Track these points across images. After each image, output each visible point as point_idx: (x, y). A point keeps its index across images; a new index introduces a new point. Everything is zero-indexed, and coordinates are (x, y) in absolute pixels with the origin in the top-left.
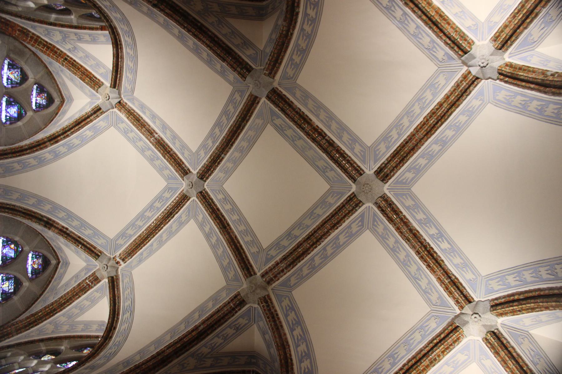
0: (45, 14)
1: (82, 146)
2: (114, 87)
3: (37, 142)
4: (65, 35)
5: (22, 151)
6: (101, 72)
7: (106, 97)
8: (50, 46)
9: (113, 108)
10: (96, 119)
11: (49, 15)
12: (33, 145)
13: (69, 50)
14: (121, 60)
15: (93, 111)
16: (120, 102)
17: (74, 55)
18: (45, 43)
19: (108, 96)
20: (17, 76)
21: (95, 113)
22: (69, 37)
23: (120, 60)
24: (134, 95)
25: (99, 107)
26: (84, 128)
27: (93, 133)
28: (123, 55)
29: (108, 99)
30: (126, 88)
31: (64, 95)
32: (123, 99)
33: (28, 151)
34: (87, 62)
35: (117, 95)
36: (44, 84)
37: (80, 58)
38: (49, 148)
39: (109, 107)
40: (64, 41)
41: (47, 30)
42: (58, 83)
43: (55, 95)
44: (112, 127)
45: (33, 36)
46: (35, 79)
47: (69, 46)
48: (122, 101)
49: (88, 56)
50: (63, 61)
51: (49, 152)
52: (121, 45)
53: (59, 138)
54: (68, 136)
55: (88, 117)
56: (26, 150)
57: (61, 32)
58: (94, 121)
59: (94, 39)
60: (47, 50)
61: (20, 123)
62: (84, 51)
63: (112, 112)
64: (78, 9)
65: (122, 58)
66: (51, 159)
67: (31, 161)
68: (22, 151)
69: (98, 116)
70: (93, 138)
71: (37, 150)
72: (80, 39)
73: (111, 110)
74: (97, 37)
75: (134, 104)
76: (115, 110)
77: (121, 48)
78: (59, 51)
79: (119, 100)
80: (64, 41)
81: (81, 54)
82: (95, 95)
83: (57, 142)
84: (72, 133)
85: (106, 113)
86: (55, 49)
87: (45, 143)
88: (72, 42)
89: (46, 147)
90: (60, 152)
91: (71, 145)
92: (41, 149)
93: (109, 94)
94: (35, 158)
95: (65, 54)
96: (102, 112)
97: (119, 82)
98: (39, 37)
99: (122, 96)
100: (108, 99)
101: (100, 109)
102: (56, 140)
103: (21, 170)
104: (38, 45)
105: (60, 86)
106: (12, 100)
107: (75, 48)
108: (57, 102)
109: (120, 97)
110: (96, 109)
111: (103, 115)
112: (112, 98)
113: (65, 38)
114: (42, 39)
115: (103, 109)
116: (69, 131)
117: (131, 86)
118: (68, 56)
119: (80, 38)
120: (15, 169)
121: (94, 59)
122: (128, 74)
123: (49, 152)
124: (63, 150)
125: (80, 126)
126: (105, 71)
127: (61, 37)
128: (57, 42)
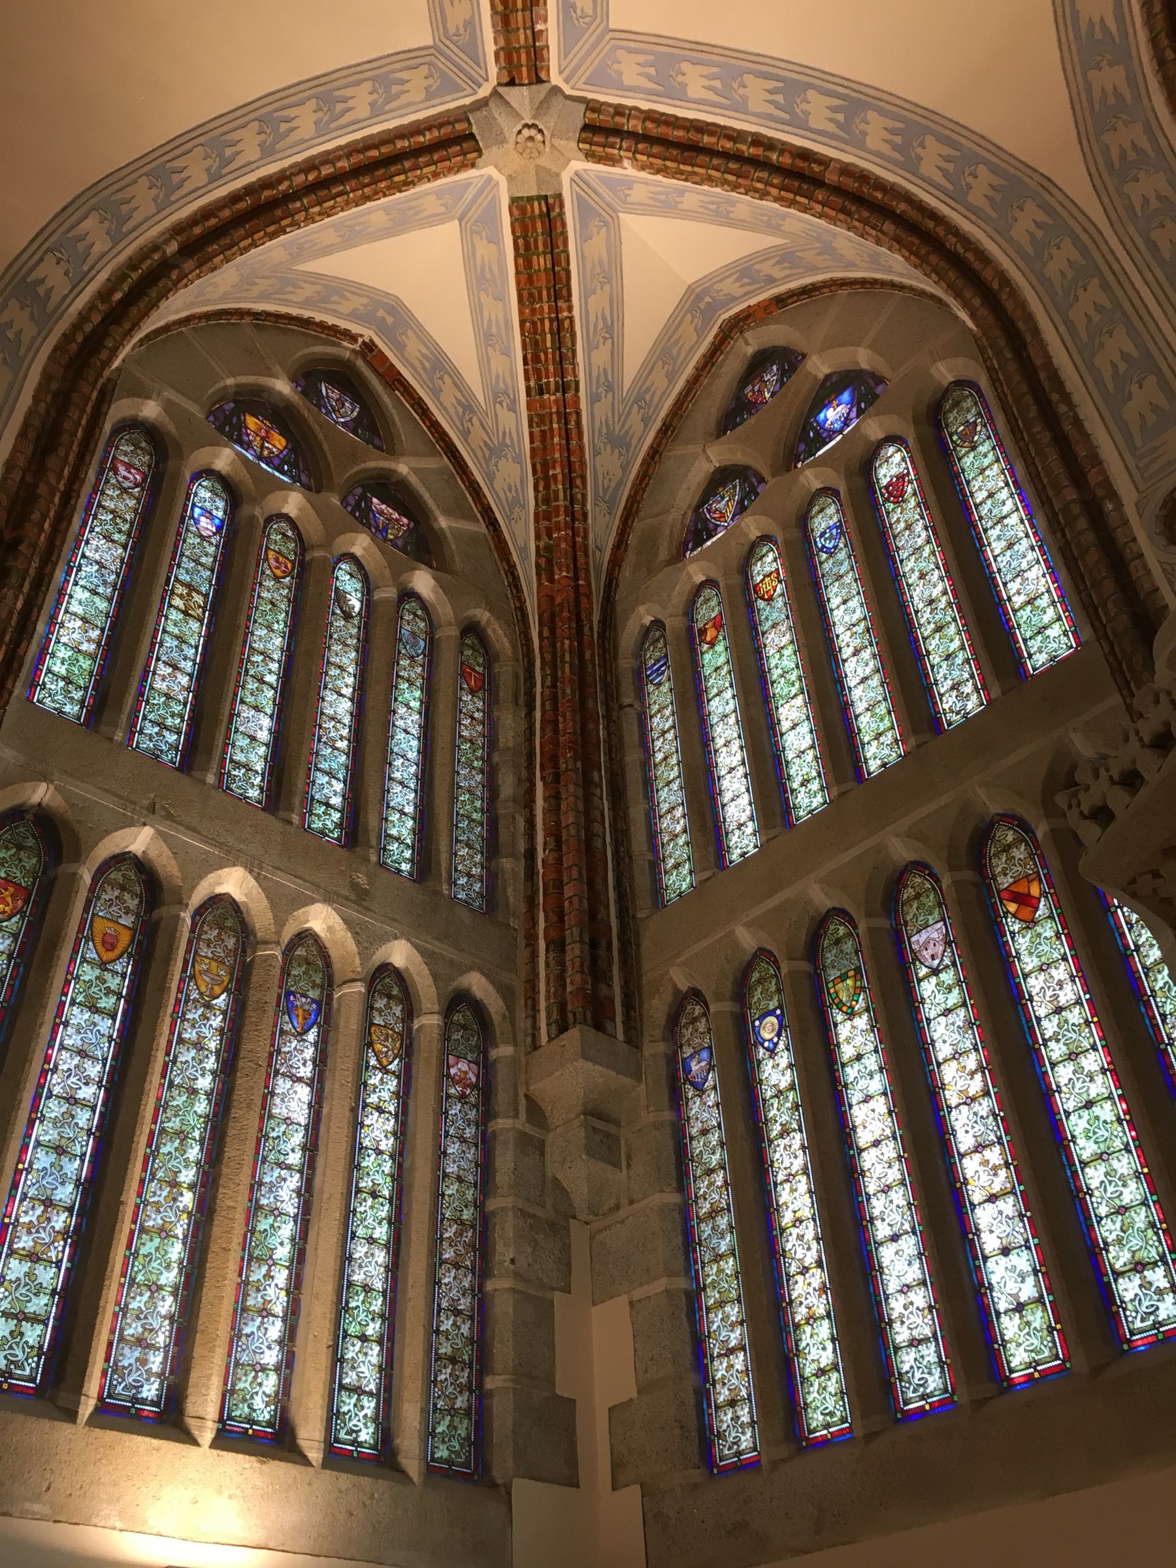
0: (453, 547)
1: (755, 58)
2: (472, 136)
3: (848, 213)
4: (487, 461)
5: (913, 228)
6: (493, 247)
7: (531, 138)
8: (538, 467)
9: (556, 90)
10: (631, 109)
11: (448, 535)
12: (866, 214)
13: (513, 408)
14: (325, 162)
15: (611, 139)
16: (512, 83)
17: (513, 376)
18: (541, 488)
19: (521, 138)
20: (723, 498)
21: (618, 132)
22: (486, 444)
23: (326, 171)
24: (431, 43)
25: (584, 135)
26: (691, 115)
27: (685, 67)
28: (291, 167)
29: (534, 126)
30: (430, 95)
31: (710, 338)
32: (493, 81)
33: (902, 207)
34: (501, 320)
35: (496, 111)
36: (713, 420)
37: (507, 353)
38: (847, 158)
39: (558, 103)
40: (503, 445)
41: (509, 519)
42: (680, 384)
43: (731, 366)
44: (612, 26)
45: (543, 532)
46: (704, 451)
47: (507, 419)
48: (506, 79)
49: (486, 338)
50: (548, 392)
51: (858, 142)
52: (250, 190)
53: (786, 160)
54: (758, 140)
55: (646, 138)
56: (900, 220)
57: (490, 477)
58: (645, 106)
59: (434, 369)
60: (555, 461)
61: (864, 358)
62: (484, 363)
63: (567, 81)
64: (325, 446)
65: (310, 165)
66: (882, 113)
67: (929, 168)
68: (913, 228)
69: (619, 110)
70: (698, 51)
71: (880, 185)
72: (468, 407)
73: (568, 91)
74: (424, 368)
75: (472, 24)
76: (556, 79)
77: (267, 183)
78: (536, 430)
79: (502, 90)
80: (503, 445)
81: (498, 364)
82: (583, 207)
83: (805, 155)
84: (736, 136)
85: (590, 96)
86: (537, 444)
87: (838, 190)
88: (490, 422)
89: (846, 170)
90: (835, 110)
91: (780, 98)
92: (864, 177)
93: (512, 139)
94: (911, 165)
95: (529, 407)
96: (594, 110)
97: (429, 129)
98: (536, 515)
99: (484, 91)
100: (534, 126)
101: (586, 128)
102: (800, 163)
103: (986, 162)
104: (557, 499)
105: (689, 371)
106: (802, 447)
107: (500, 395)
108: (749, 344)
109: (495, 93)
110: (596, 139)
111: (602, 98)
112: (518, 116)
113: (494, 451)
114: (537, 505)
115: (578, 115)
116: (738, 157)
117: (405, 75)
118: (528, 389)
119: (464, 413)
120: (997, 181)
121: (476, 309)
122: (361, 109)
123: (858, 142)
124: (818, 109)
125: (693, 136)
126: (476, 238)
127: (502, 463)
128: (518, 460)
